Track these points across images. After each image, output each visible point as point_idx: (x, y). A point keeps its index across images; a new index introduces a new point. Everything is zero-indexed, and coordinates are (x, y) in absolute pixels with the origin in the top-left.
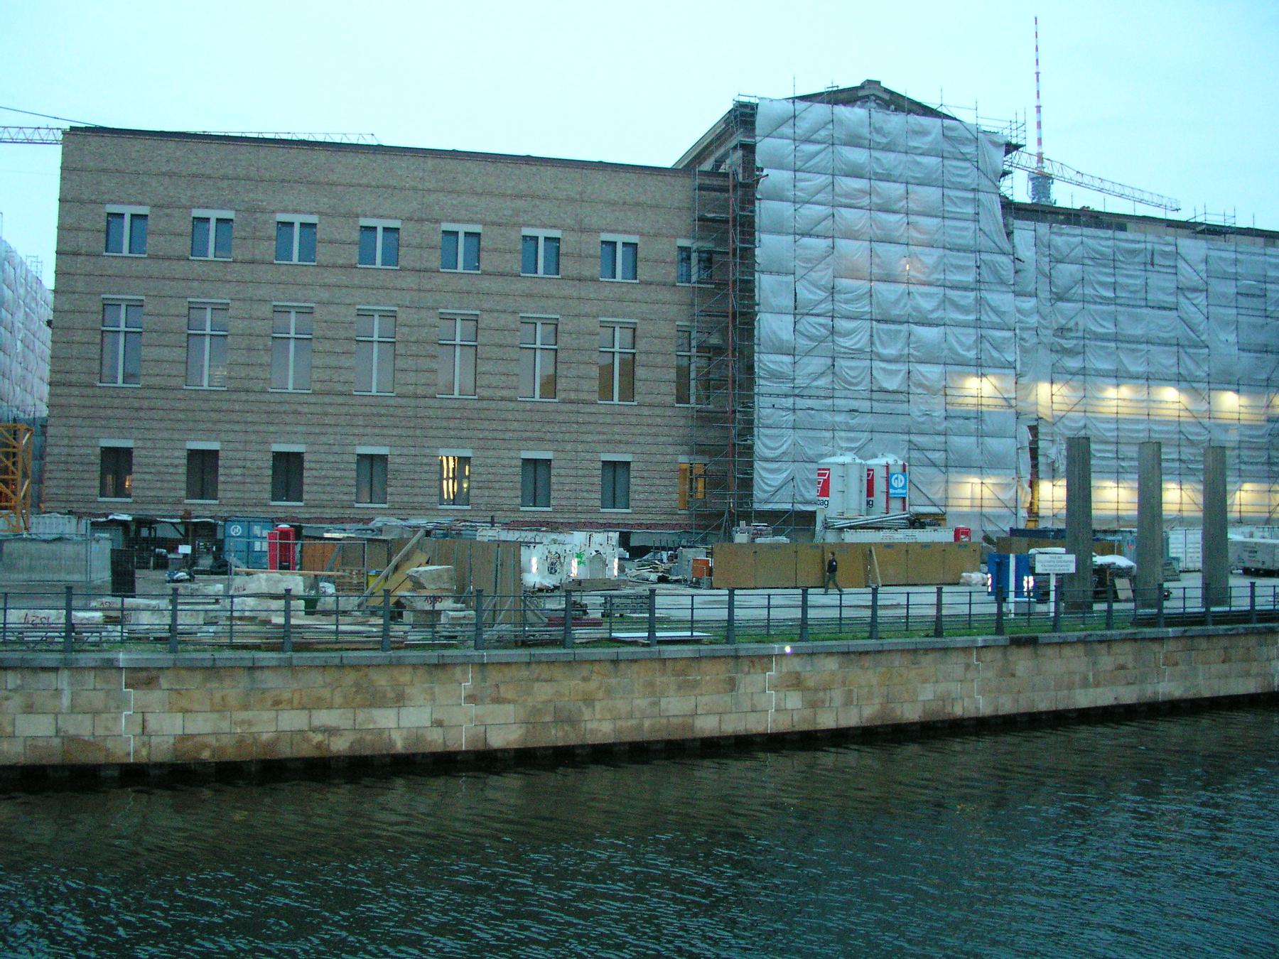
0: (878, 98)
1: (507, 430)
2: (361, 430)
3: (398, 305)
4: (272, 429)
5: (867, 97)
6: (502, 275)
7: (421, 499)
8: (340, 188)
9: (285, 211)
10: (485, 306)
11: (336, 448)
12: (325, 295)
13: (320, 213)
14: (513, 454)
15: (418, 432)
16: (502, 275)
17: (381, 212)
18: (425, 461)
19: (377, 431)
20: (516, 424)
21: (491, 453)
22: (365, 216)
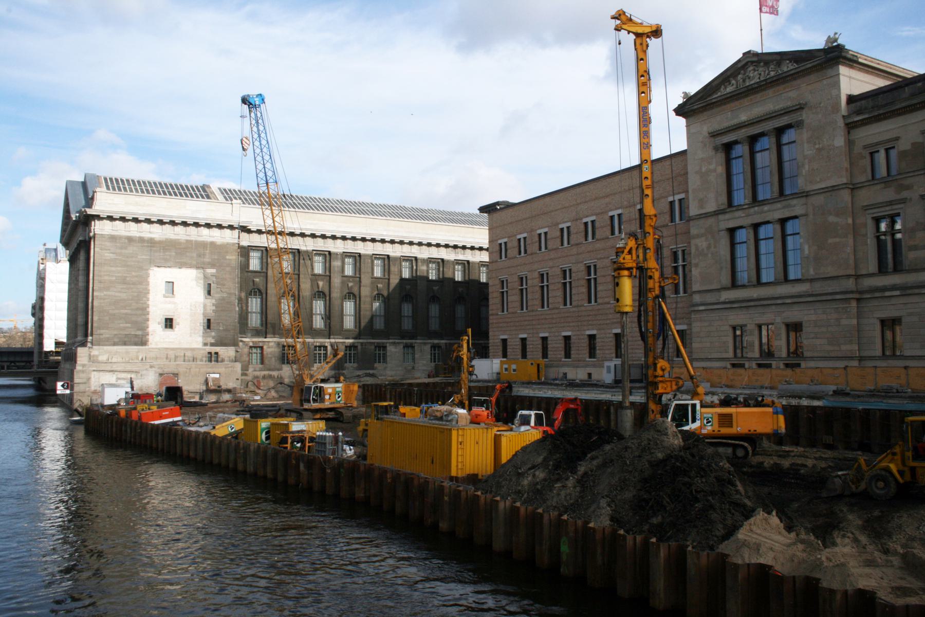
0: (752, 62)
1: (607, 319)
2: (562, 325)
3: (571, 263)
4: (539, 327)
5: (746, 64)
6: (603, 239)
7: (581, 356)
8: (553, 214)
9: (539, 229)
10: (599, 256)
11: (557, 334)
12: (551, 264)
13: (548, 227)
14: (610, 331)
15: (579, 323)
16: (603, 239)
17: (565, 220)
18: (582, 337)
19: (567, 324)
20: (610, 315)
21: (603, 331)
22: (561, 223)
